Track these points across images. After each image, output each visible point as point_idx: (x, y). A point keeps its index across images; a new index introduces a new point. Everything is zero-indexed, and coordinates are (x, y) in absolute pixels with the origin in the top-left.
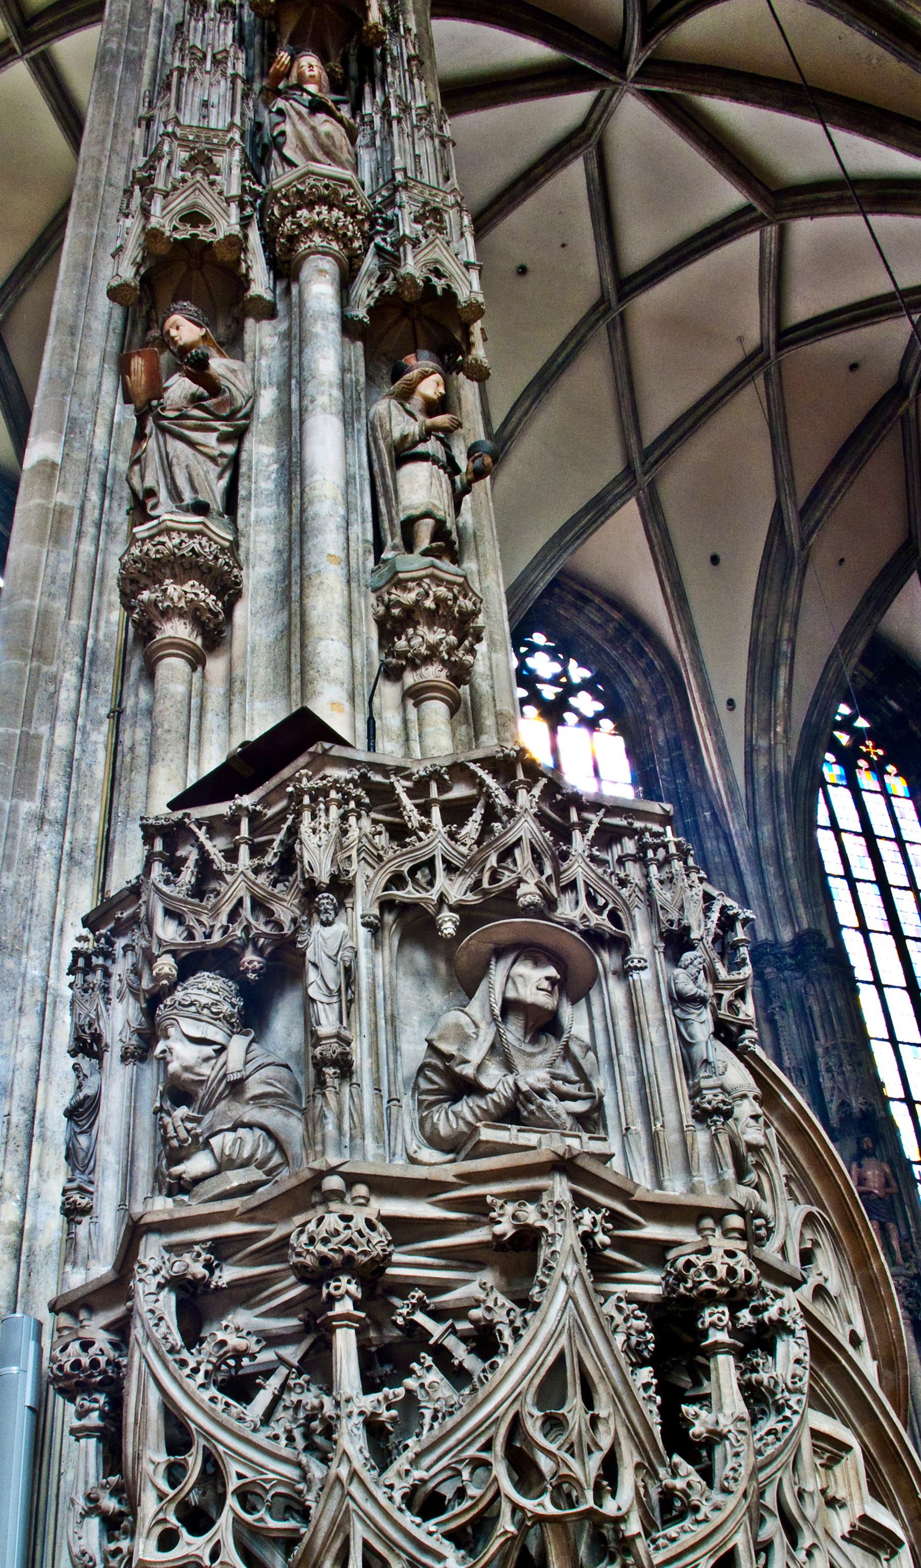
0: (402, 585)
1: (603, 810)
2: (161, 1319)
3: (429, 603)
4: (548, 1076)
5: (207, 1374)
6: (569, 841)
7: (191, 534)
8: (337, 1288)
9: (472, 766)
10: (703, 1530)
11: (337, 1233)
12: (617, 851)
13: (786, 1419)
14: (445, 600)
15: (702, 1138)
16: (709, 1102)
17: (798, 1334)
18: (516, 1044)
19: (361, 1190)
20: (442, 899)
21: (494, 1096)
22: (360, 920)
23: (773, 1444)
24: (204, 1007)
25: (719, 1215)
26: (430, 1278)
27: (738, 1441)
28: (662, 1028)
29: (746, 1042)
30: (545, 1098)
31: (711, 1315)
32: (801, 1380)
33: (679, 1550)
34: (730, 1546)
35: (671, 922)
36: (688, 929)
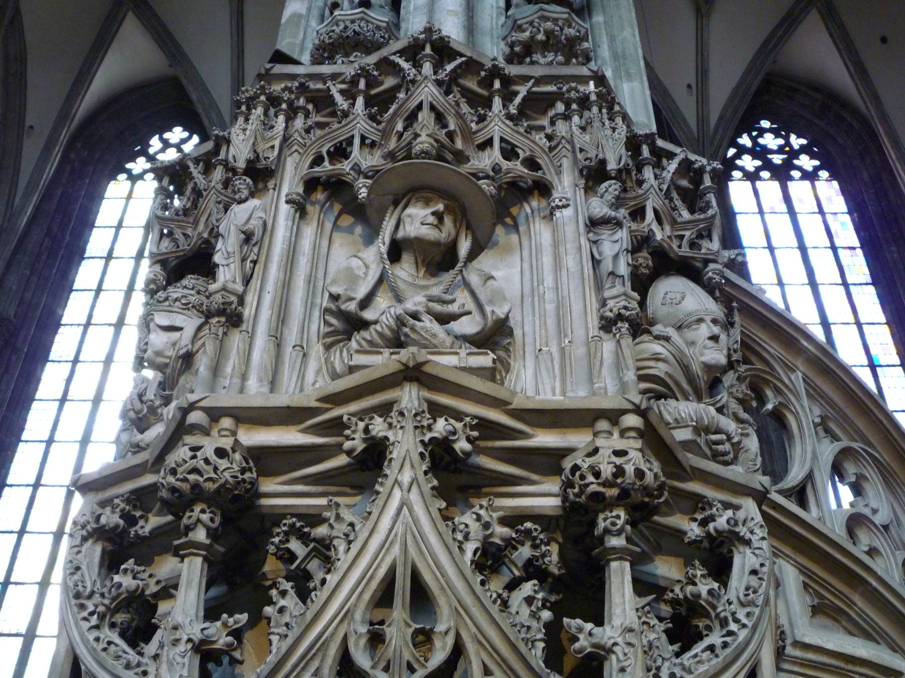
0: (520, 29)
1: (533, 81)
2: (78, 568)
3: (541, 37)
4: (424, 299)
5: (102, 617)
6: (488, 105)
7: (353, 22)
9: (393, 58)
12: (551, 113)
13: (730, 633)
14: (553, 31)
16: (611, 311)
17: (756, 544)
18: (410, 280)
21: (378, 327)
22: (283, 199)
23: (709, 660)
24: (176, 300)
25: (613, 416)
26: (309, 506)
27: (625, 654)
28: (578, 255)
29: (710, 274)
30: (420, 320)
31: (605, 519)
32: (755, 592)
36: (603, 162)
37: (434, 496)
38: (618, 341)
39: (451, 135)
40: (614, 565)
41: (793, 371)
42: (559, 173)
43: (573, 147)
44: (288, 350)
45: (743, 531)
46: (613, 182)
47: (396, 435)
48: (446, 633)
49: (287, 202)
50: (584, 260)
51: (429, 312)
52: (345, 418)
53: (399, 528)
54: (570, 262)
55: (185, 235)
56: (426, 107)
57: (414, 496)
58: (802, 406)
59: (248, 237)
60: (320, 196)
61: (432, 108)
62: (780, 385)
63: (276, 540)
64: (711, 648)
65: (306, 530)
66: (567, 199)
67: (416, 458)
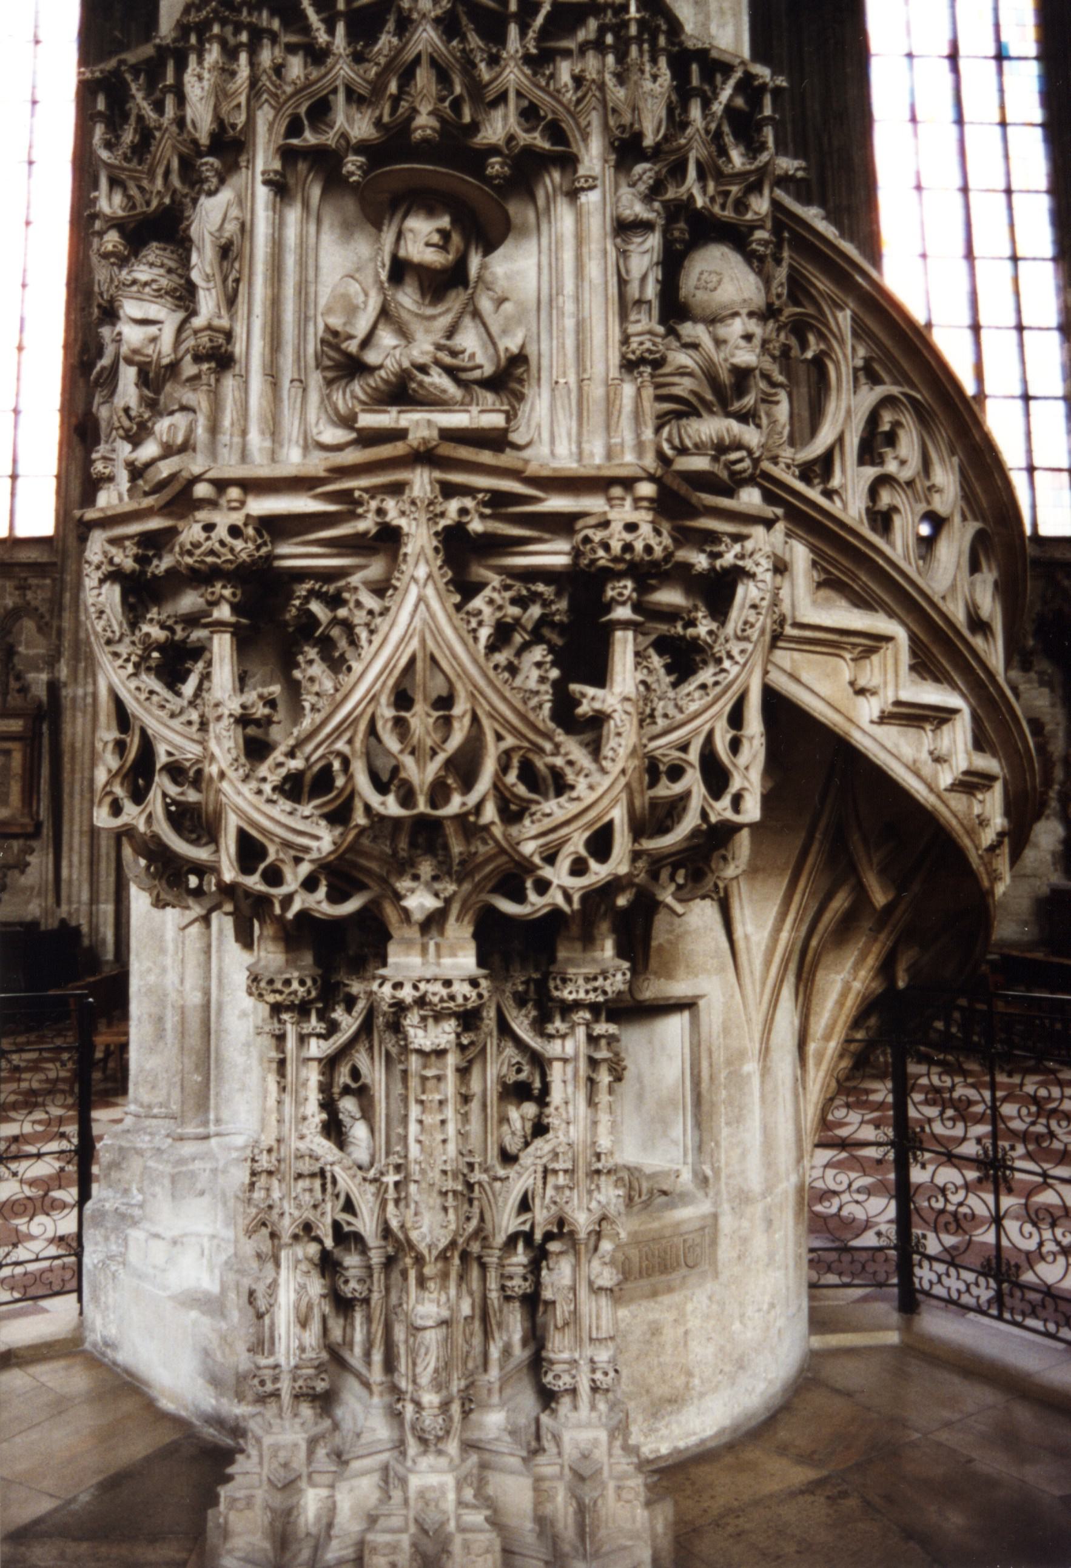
2: (102, 612)
4: (431, 348)
5: (137, 666)
8: (213, 593)
10: (574, 808)
11: (197, 545)
12: (582, 35)
15: (628, 390)
16: (633, 352)
17: (759, 577)
19: (234, 493)
20: (344, 136)
21: (382, 373)
22: (259, 178)
24: (146, 284)
25: (628, 483)
29: (754, 246)
30: (427, 374)
31: (613, 589)
33: (551, 826)
34: (606, 819)
35: (622, 127)
36: (639, 136)
37: (449, 591)
38: (639, 390)
39: (456, 105)
40: (619, 634)
41: (842, 309)
42: (585, 137)
43: (605, 106)
44: (286, 384)
45: (748, 564)
46: (646, 166)
47: (409, 525)
48: (463, 716)
49: (266, 183)
50: (609, 273)
51: (437, 362)
52: (357, 494)
53: (417, 622)
54: (593, 269)
55: (141, 189)
56: (425, 60)
57: (430, 592)
58: (845, 355)
59: (226, 251)
60: (302, 167)
61: (434, 63)
62: (824, 330)
63: (297, 602)
64: (703, 687)
65: (324, 589)
66: (595, 178)
67: (430, 553)
